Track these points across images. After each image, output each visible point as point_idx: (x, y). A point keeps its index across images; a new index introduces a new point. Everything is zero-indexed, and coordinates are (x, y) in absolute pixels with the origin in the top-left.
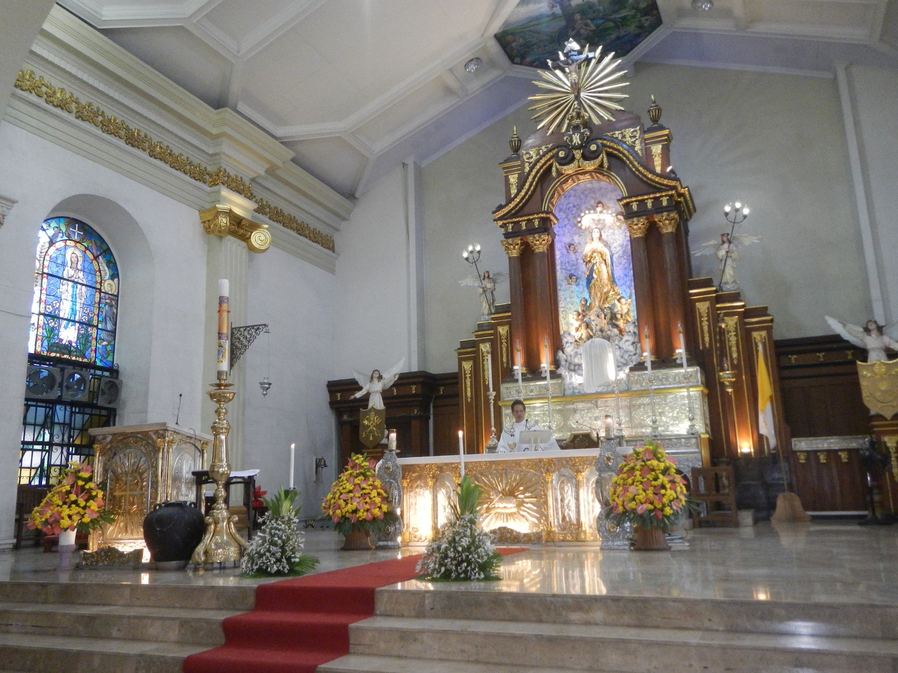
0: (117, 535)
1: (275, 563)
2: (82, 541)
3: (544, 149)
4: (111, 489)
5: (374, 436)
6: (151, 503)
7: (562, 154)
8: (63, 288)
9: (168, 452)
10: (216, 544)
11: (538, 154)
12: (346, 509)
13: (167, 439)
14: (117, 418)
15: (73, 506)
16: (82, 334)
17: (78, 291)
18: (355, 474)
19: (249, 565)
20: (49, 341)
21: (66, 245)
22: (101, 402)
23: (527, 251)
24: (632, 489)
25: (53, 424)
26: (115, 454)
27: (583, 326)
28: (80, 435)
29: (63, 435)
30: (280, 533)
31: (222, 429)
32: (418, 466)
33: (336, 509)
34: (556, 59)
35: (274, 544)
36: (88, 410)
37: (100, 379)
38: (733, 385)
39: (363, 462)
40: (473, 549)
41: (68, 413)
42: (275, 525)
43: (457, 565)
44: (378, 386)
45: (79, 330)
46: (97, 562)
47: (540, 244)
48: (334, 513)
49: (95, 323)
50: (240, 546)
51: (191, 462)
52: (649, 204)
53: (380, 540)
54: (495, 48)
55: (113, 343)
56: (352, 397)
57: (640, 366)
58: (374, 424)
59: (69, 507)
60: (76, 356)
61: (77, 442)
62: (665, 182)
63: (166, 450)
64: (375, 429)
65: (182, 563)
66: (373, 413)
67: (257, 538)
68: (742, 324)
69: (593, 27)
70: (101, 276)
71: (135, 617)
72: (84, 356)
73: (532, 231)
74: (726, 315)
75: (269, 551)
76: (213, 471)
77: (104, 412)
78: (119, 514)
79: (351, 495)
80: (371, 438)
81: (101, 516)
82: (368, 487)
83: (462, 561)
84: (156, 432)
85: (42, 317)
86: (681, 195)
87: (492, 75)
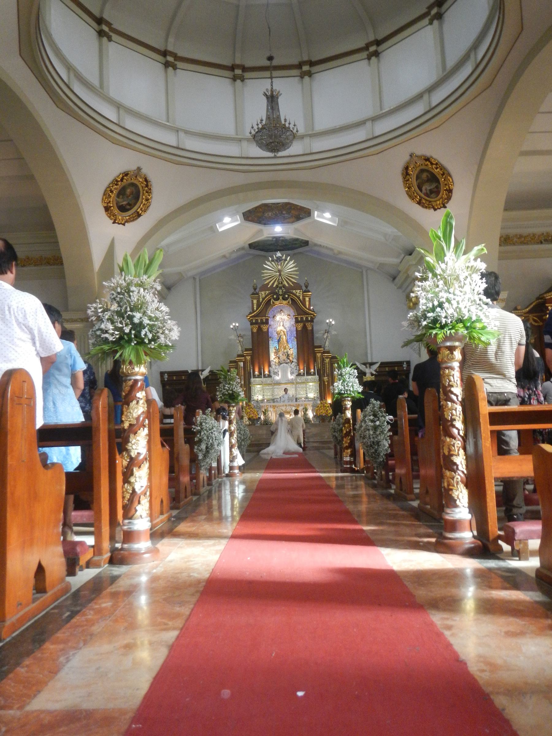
3: (267, 292)
7: (275, 296)
11: (265, 294)
23: (260, 329)
24: (321, 411)
27: (277, 358)
34: (272, 257)
38: (328, 382)
47: (264, 328)
52: (304, 319)
54: (247, 246)
57: (299, 375)
62: (310, 312)
68: (330, 361)
69: (284, 244)
73: (262, 323)
74: (326, 358)
86: (314, 316)
87: (243, 252)
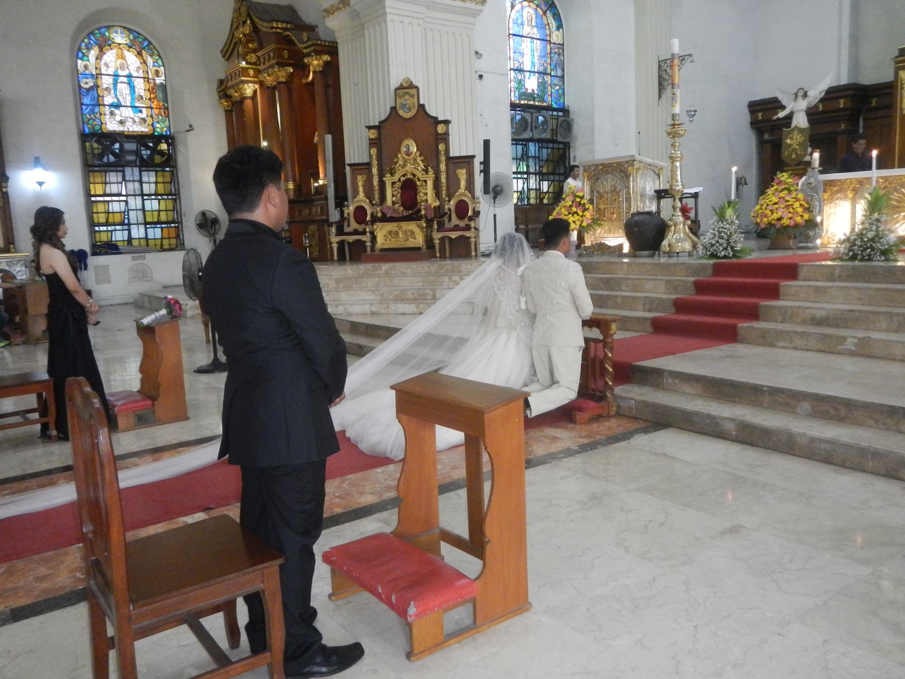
0: (603, 235)
1: (723, 250)
2: (581, 238)
4: (597, 204)
5: (796, 154)
6: (626, 213)
8: (524, 45)
9: (637, 176)
10: (676, 239)
12: (772, 217)
13: (635, 167)
14: (571, 150)
15: (575, 215)
16: (541, 83)
17: (535, 46)
18: (780, 189)
19: (704, 251)
20: (519, 91)
21: (522, 7)
22: (560, 139)
25: (528, 157)
26: (598, 179)
28: (546, 164)
29: (535, 165)
30: (726, 231)
31: (677, 158)
32: (839, 181)
33: (762, 218)
35: (722, 238)
36: (551, 145)
37: (557, 119)
39: (787, 179)
40: (877, 239)
41: (537, 148)
42: (722, 225)
43: (862, 251)
44: (802, 105)
45: (538, 78)
46: (593, 252)
48: (761, 220)
49: (549, 71)
50: (693, 241)
51: (651, 183)
53: (801, 242)
55: (562, 87)
56: (775, 118)
58: (797, 143)
59: (573, 216)
60: (538, 102)
61: (545, 171)
63: (634, 175)
64: (797, 147)
65: (651, 252)
66: (796, 132)
67: (709, 234)
70: (549, 28)
71: (636, 279)
72: (543, 101)
75: (718, 242)
76: (671, 189)
77: (561, 146)
78: (603, 220)
79: (776, 206)
80: (794, 156)
81: (592, 222)
82: (791, 200)
83: (867, 248)
84: (627, 162)
85: (512, 71)
